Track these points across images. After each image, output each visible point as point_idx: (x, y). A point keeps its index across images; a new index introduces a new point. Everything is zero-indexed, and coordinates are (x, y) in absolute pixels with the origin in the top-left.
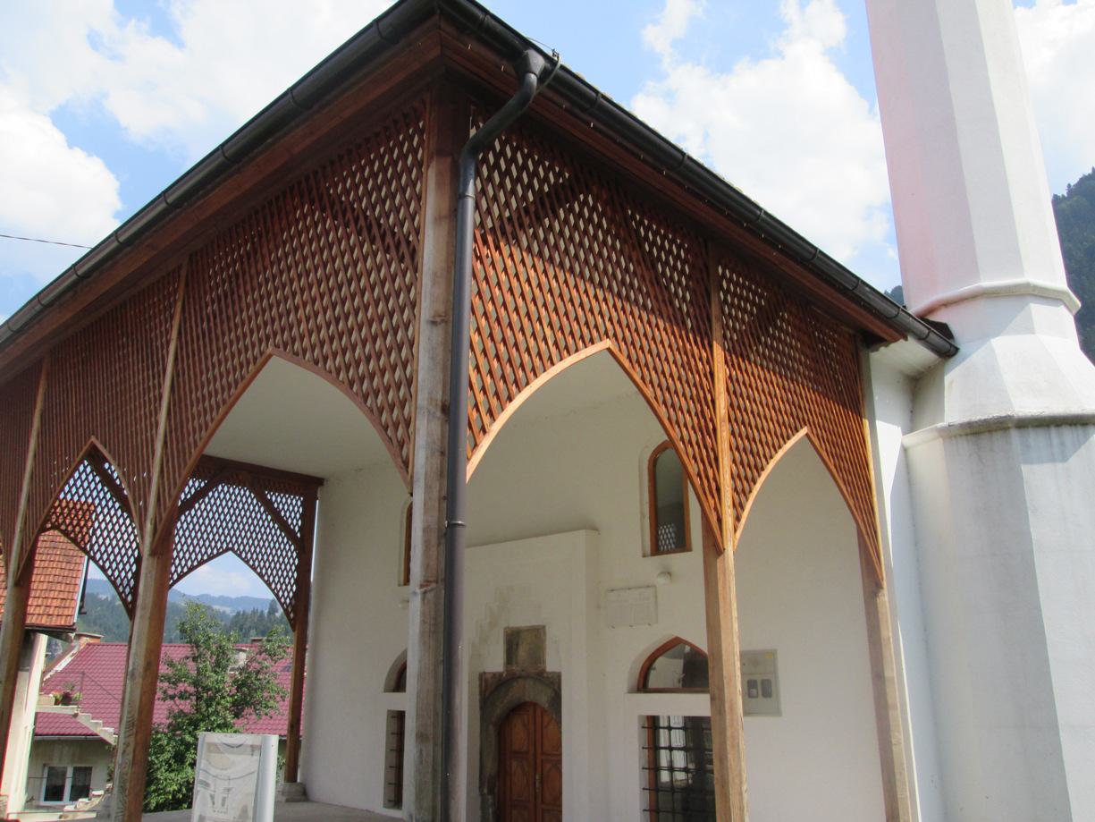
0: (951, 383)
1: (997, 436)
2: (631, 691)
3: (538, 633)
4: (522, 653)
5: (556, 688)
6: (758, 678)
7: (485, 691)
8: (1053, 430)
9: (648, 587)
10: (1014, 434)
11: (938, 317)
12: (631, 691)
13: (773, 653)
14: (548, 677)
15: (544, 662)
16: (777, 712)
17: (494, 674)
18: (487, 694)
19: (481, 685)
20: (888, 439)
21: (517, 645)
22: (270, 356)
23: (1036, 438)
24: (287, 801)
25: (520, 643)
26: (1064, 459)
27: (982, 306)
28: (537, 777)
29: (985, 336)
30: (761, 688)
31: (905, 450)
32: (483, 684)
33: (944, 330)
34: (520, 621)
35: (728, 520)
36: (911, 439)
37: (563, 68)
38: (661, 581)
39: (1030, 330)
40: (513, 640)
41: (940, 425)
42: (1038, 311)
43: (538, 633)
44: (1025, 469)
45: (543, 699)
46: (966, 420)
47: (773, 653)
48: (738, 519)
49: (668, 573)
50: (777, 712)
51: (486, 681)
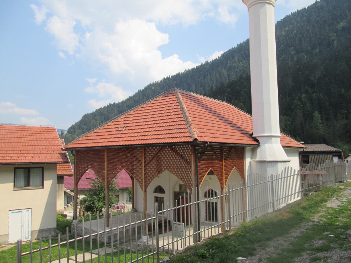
0: (258, 152)
1: (264, 163)
4: (183, 188)
8: (272, 163)
9: (207, 180)
10: (267, 164)
11: (258, 138)
17: (177, 192)
18: (176, 195)
20: (248, 161)
22: (165, 170)
23: (270, 164)
24: (134, 212)
26: (273, 167)
27: (265, 138)
29: (264, 144)
31: (250, 162)
33: (257, 141)
35: (224, 186)
36: (251, 161)
37: (209, 142)
38: (209, 180)
39: (271, 143)
41: (256, 160)
42: (273, 139)
44: (267, 168)
46: (259, 160)
48: (225, 184)
49: (210, 179)
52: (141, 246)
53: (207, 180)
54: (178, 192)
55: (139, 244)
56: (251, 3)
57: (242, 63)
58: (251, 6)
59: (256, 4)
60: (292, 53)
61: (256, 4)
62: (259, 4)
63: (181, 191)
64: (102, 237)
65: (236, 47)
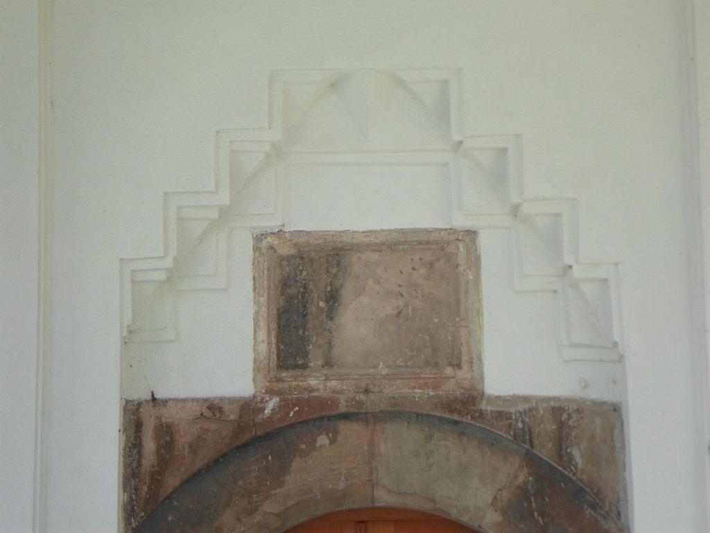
3: (441, 260)
5: (545, 451)
7: (157, 478)
14: (500, 415)
15: (476, 362)
17: (214, 408)
18: (172, 482)
19: (133, 447)
21: (333, 298)
25: (347, 292)
32: (149, 445)
34: (362, 193)
40: (304, 286)
43: (441, 260)
45: (475, 487)
51: (166, 434)
54: (248, 407)
63: (317, 382)
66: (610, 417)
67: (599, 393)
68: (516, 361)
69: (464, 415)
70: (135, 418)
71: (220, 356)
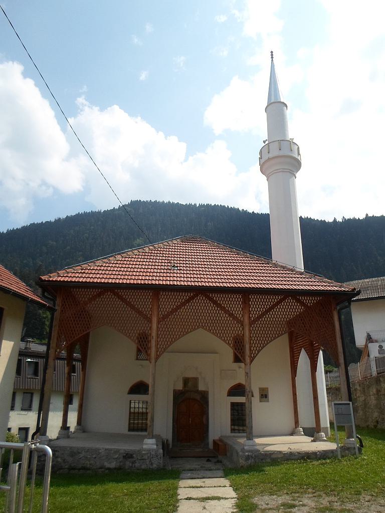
2: (228, 396)
3: (196, 380)
4: (190, 384)
6: (264, 394)
9: (235, 370)
12: (228, 396)
13: (267, 388)
16: (268, 401)
17: (179, 390)
28: (190, 419)
30: (264, 396)
34: (191, 374)
40: (186, 381)
43: (196, 380)
45: (198, 397)
47: (267, 388)
50: (268, 401)
51: (176, 392)
52: (252, 457)
53: (235, 370)
54: (182, 390)
55: (248, 456)
56: (280, 169)
57: (11, 256)
58: (280, 172)
59: (278, 172)
60: (79, 259)
61: (272, 174)
62: (288, 173)
63: (187, 389)
64: (145, 459)
65: (5, 232)
66: (208, 392)
67: (207, 390)
68: (201, 388)
69: (198, 392)
70: (174, 390)
71: (180, 387)
